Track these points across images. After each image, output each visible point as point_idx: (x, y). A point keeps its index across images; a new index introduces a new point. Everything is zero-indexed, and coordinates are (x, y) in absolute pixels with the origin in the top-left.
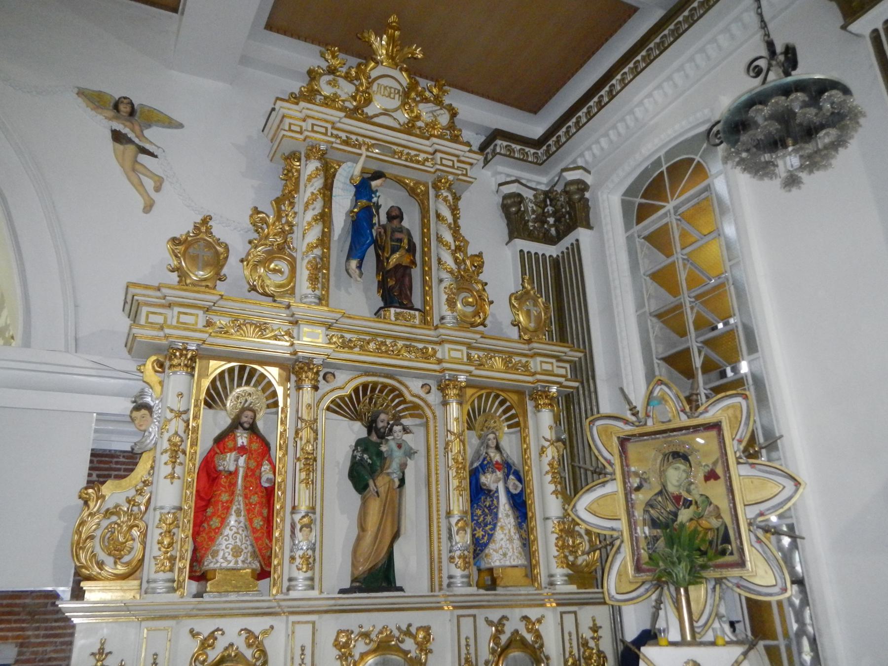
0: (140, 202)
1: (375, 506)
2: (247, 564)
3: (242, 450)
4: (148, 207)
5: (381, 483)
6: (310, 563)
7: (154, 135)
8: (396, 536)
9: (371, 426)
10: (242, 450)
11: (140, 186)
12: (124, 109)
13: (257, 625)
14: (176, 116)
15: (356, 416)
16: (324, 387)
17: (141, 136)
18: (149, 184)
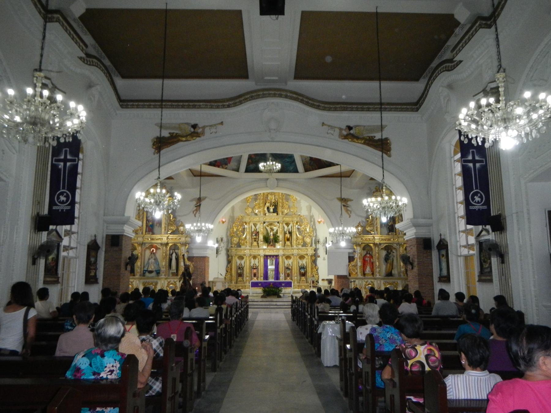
0: (348, 216)
1: (388, 265)
2: (371, 273)
3: (368, 257)
4: (350, 217)
5: (390, 261)
6: (379, 273)
7: (349, 203)
8: (392, 269)
9: (388, 252)
10: (368, 257)
11: (348, 213)
12: (344, 200)
13: (373, 280)
14: (352, 199)
15: (385, 250)
16: (379, 247)
17: (347, 204)
18: (349, 212)
